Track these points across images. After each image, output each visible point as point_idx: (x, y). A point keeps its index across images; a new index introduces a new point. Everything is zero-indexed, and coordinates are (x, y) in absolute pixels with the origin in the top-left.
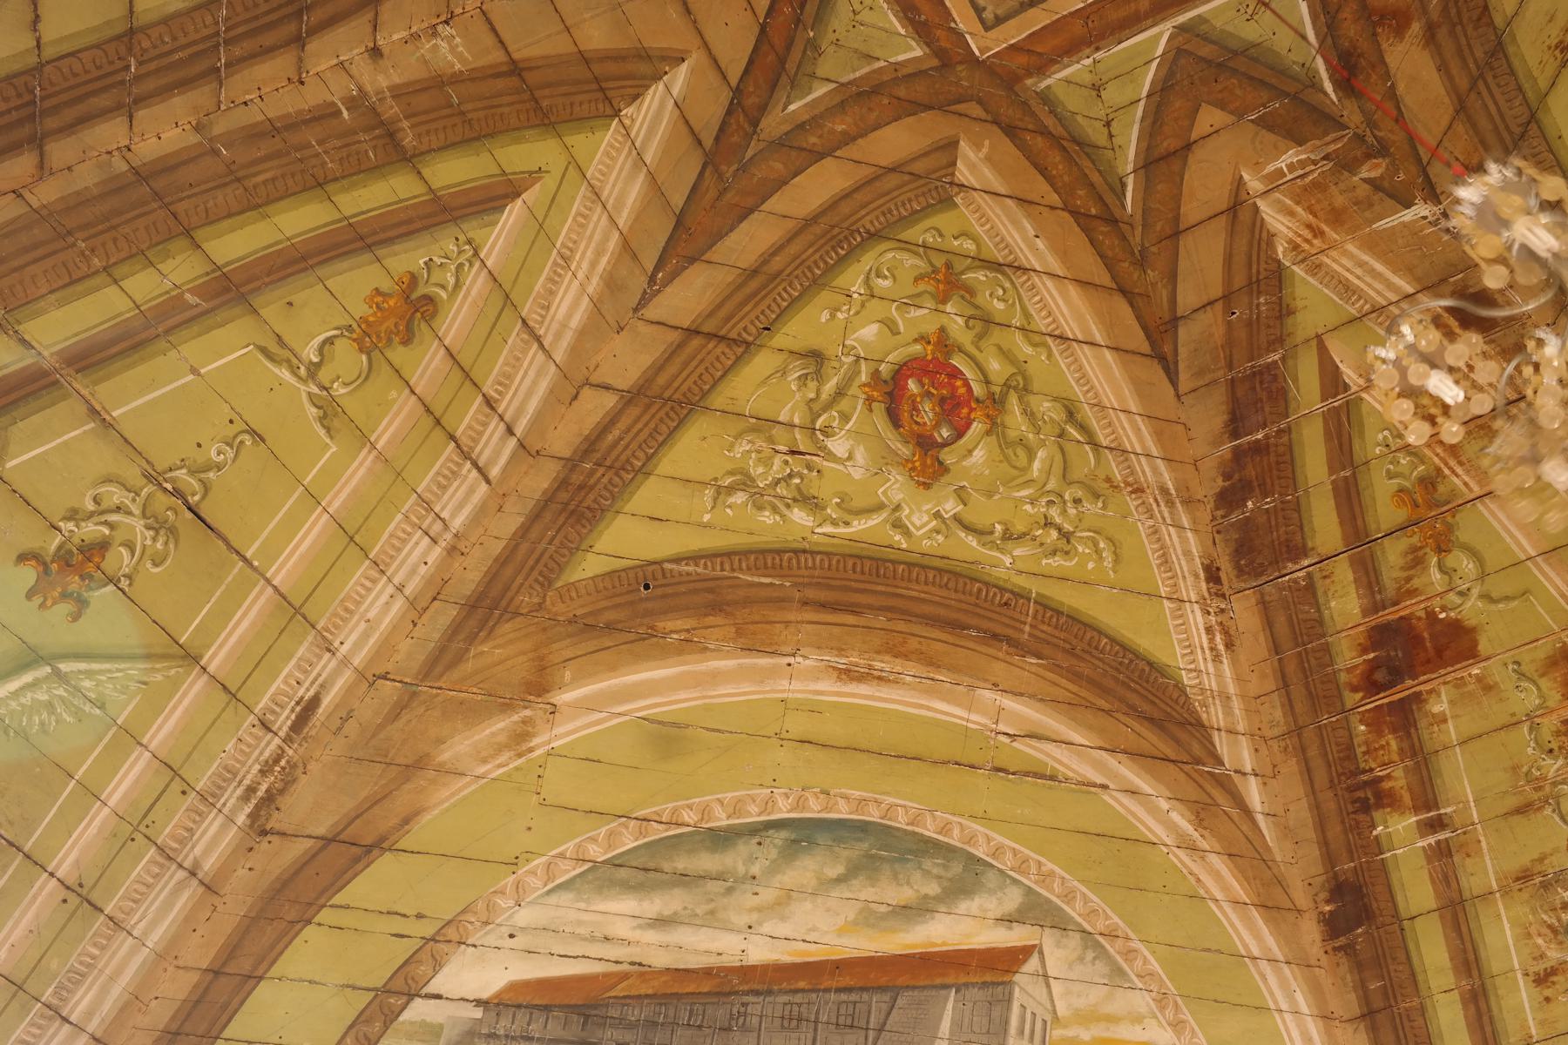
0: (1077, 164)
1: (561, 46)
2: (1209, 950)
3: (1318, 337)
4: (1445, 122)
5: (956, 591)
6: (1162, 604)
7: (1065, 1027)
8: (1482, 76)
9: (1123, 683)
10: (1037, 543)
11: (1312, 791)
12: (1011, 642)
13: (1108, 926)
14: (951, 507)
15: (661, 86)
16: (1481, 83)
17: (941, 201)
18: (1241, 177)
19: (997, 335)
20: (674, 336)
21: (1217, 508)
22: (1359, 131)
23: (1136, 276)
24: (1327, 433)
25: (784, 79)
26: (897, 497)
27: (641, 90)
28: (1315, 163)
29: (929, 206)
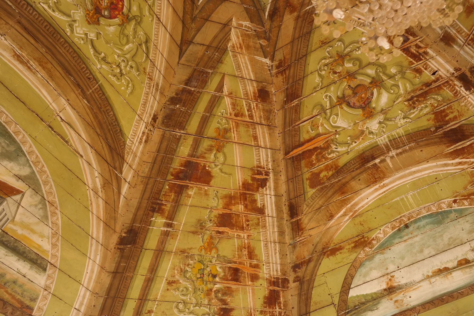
2: (80, 227)
3: (224, 74)
5: (76, 62)
6: (135, 116)
7: (15, 225)
8: (302, 37)
9: (109, 129)
10: (112, 69)
11: (142, 198)
12: (82, 90)
13: (53, 200)
14: (92, 36)
16: (300, 39)
18: (232, 19)
21: (168, 101)
22: (266, 31)
26: (77, 18)
28: (252, 30)
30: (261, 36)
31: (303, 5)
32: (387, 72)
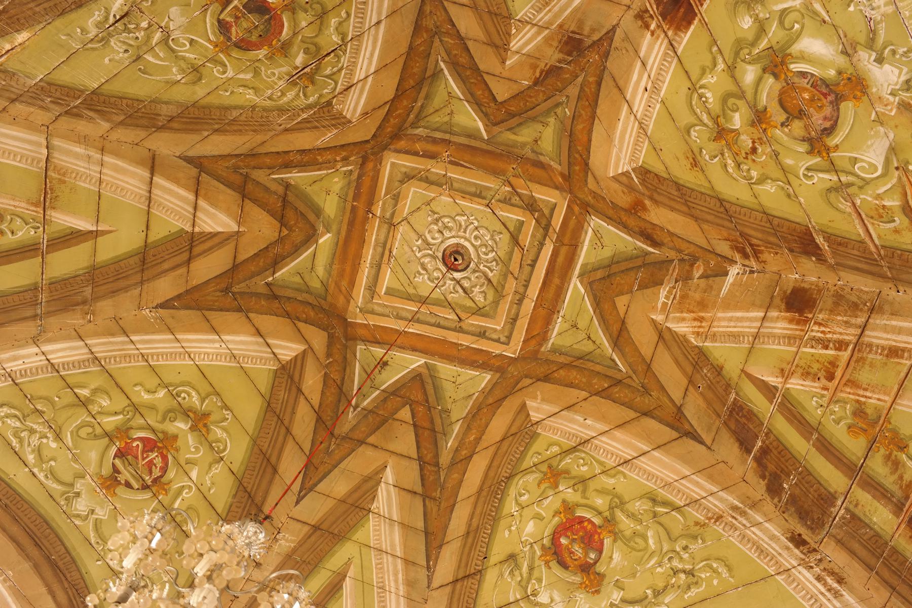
0: (585, 369)
1: (330, 503)
4: (698, 229)
6: (776, 580)
10: (676, 587)
15: (383, 485)
17: (531, 438)
18: (652, 319)
19: (592, 485)
20: (448, 589)
21: (773, 499)
23: (647, 401)
24: (787, 419)
25: (439, 436)
27: (374, 494)
28: (674, 287)
29: (527, 444)
30: (688, 271)
31: (631, 188)
32: (750, 37)
